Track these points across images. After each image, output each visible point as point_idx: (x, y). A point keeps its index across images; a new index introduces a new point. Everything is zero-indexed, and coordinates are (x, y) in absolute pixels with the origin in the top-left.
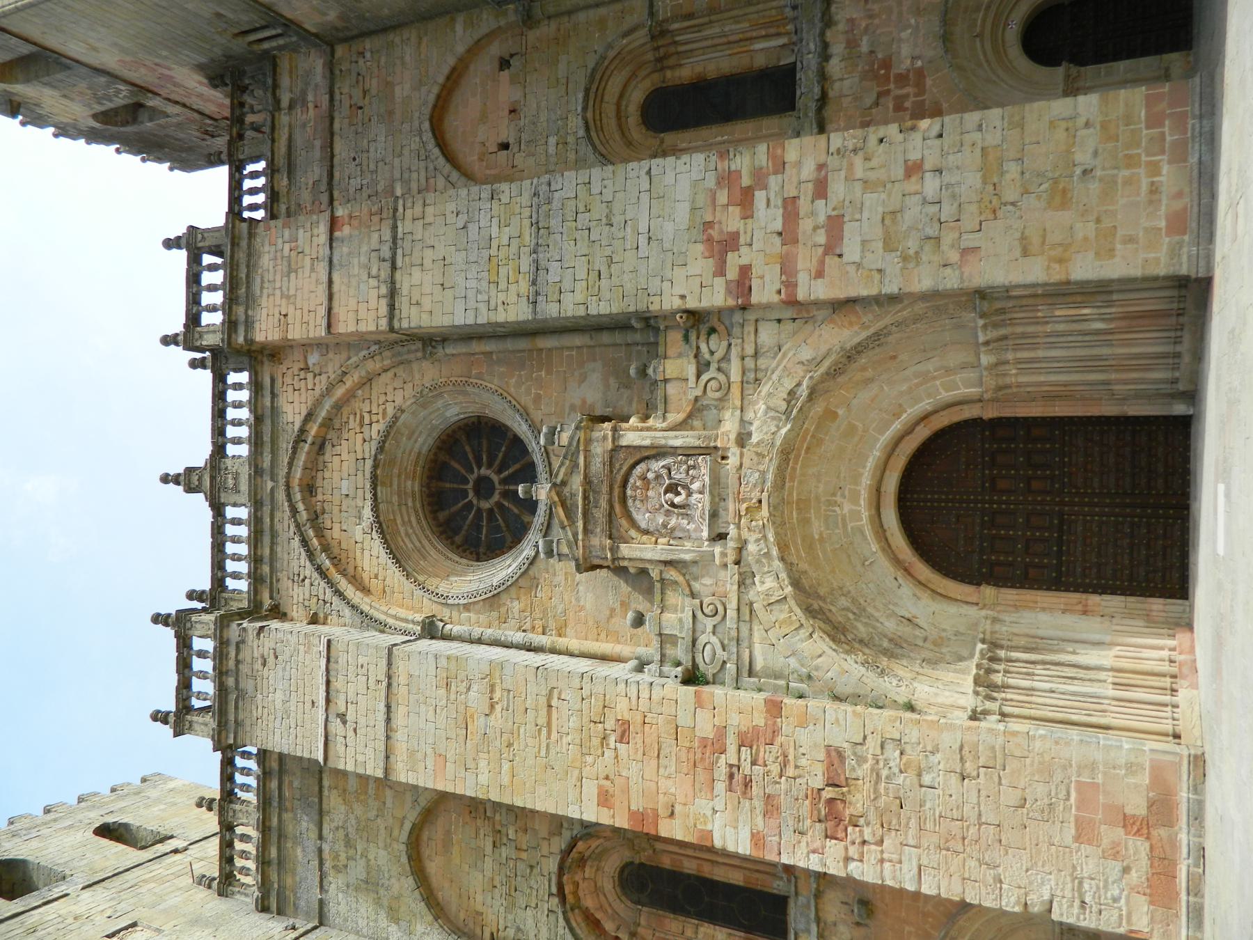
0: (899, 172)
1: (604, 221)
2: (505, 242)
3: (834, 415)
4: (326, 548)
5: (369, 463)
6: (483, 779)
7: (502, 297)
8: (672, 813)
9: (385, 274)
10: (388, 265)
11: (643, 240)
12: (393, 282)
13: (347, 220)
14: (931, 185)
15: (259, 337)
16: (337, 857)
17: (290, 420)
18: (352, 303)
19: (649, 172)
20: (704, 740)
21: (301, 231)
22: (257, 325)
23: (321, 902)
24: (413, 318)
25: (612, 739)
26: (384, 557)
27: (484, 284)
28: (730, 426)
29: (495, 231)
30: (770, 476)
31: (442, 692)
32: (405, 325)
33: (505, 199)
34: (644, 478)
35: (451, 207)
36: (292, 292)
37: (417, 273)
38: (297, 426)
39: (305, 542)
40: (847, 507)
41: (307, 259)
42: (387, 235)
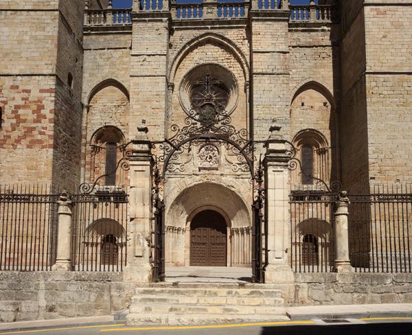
2: (275, 109)
3: (228, 196)
5: (216, 62)
6: (134, 107)
7: (260, 109)
9: (269, 71)
10: (271, 72)
12: (266, 74)
15: (254, 24)
16: (104, 55)
17: (229, 34)
18: (261, 60)
22: (257, 23)
23: (90, 49)
24: (256, 79)
26: (191, 68)
28: (227, 171)
29: (277, 106)
30: (213, 182)
31: (155, 93)
32: (254, 78)
33: (286, 109)
34: (213, 149)
35: (285, 93)
38: (226, 36)
40: (207, 199)
42: (280, 71)
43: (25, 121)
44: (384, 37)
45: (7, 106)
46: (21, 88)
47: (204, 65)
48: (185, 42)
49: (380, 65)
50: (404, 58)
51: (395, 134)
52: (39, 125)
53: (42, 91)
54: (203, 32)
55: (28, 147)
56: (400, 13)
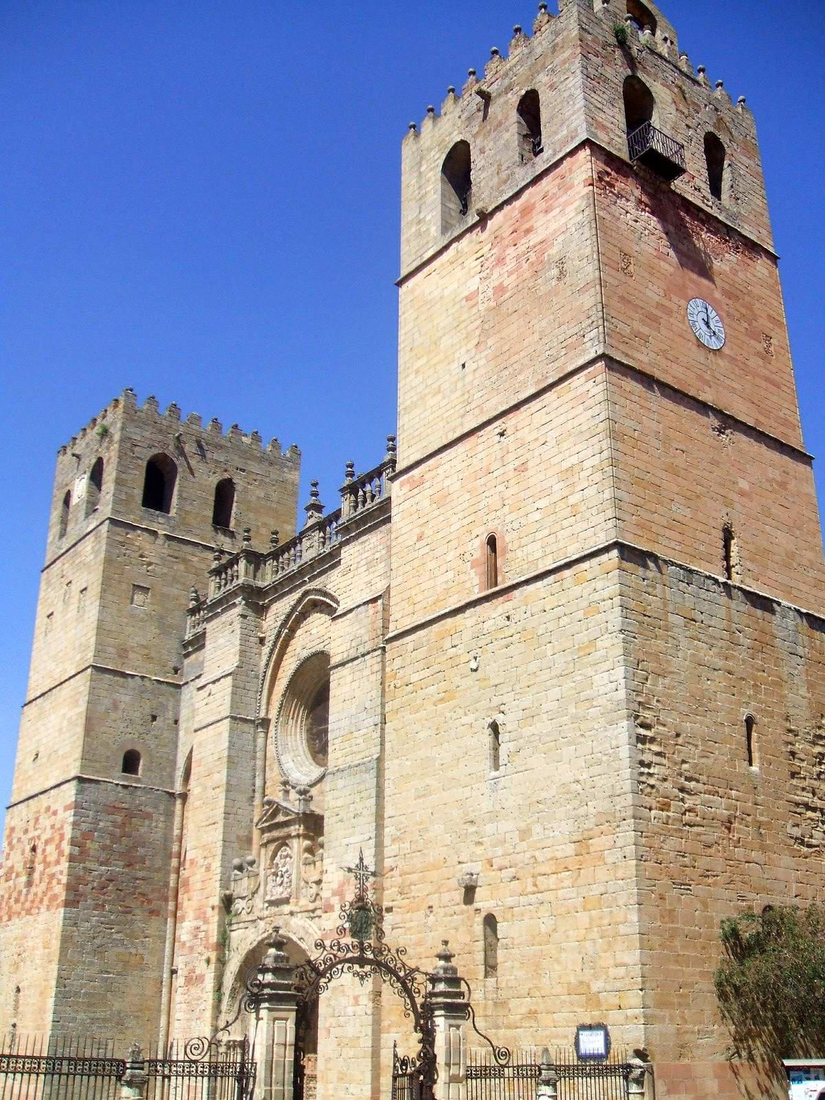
0: (357, 994)
1: (356, 812)
4: (293, 631)
7: (337, 746)
8: (189, 900)
9: (353, 654)
11: (346, 841)
13: (376, 610)
14: (350, 1010)
19: (370, 838)
20: (205, 913)
21: (383, 564)
25: (206, 863)
27: (342, 733)
29: (363, 731)
36: (360, 570)
37: (349, 678)
39: (289, 616)
41: (371, 576)
42: (368, 647)
43: (47, 864)
44: (420, 538)
45: (40, 844)
46: (51, 810)
47: (308, 659)
48: (279, 623)
49: (411, 609)
50: (450, 575)
51: (428, 781)
52: (59, 868)
53: (66, 808)
54: (296, 595)
55: (48, 908)
56: (446, 467)
